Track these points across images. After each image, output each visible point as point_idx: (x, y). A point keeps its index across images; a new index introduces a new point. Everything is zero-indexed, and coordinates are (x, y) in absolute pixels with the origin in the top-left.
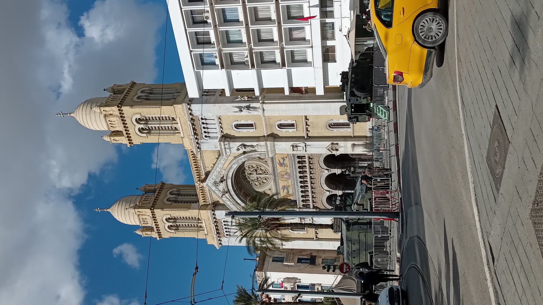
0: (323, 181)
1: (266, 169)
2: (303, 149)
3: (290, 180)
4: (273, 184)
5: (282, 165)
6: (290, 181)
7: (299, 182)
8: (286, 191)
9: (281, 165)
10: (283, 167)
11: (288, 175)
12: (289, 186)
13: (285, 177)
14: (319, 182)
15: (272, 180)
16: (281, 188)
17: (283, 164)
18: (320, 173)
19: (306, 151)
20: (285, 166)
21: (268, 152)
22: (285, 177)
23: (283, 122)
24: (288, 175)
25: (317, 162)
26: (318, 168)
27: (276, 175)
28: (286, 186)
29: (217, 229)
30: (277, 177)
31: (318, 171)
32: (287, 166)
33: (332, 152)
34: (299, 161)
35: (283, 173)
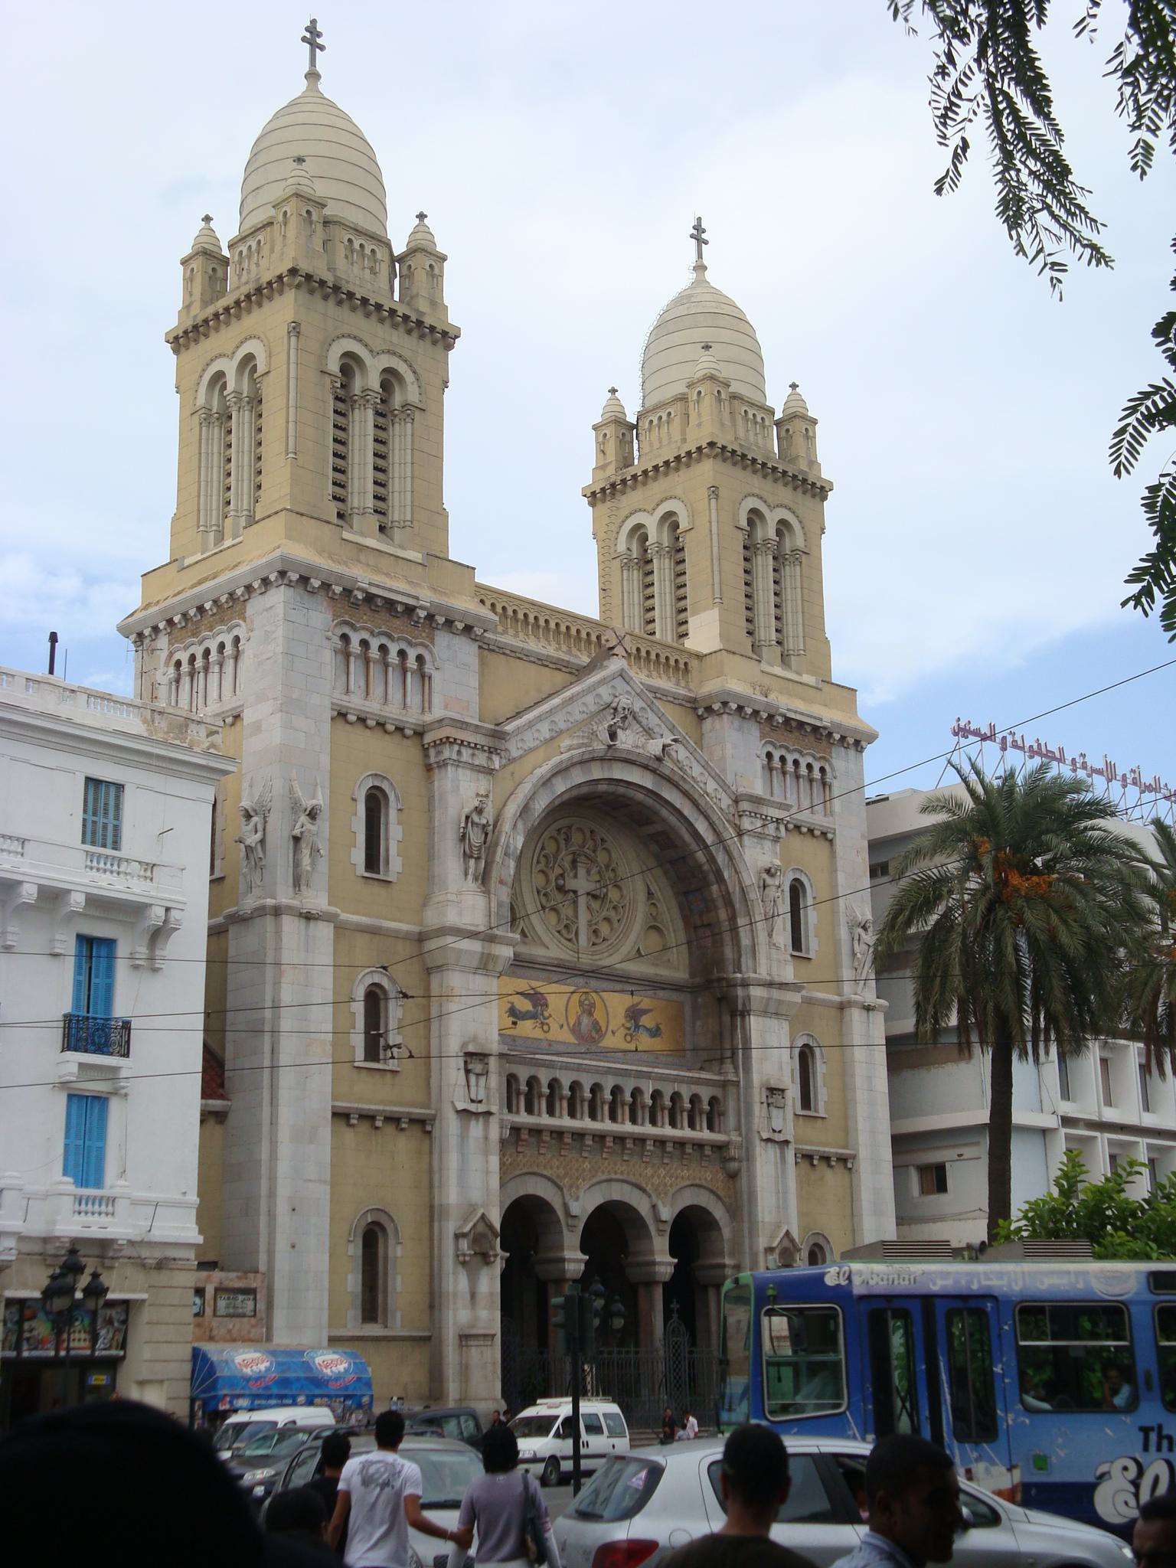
0: (619, 1193)
1: (607, 944)
2: (774, 1131)
3: (573, 1040)
4: (552, 955)
5: (632, 1018)
6: (566, 1036)
7: (619, 1081)
8: (525, 1005)
9: (634, 1015)
10: (624, 1021)
11: (594, 1034)
12: (546, 1028)
13: (585, 1020)
14: (616, 1173)
15: (568, 958)
16: (535, 984)
17: (637, 1026)
18: (653, 1185)
19: (769, 1140)
20: (629, 1029)
21: (770, 985)
22: (585, 1020)
23: (820, 1069)
24: (594, 1034)
25: (694, 1178)
26: (671, 1177)
27: (593, 983)
28: (546, 1014)
29: (390, 604)
30: (581, 981)
31: (659, 1177)
32: (628, 1038)
33: (769, 1250)
34: (560, 1086)
35: (598, 1015)
